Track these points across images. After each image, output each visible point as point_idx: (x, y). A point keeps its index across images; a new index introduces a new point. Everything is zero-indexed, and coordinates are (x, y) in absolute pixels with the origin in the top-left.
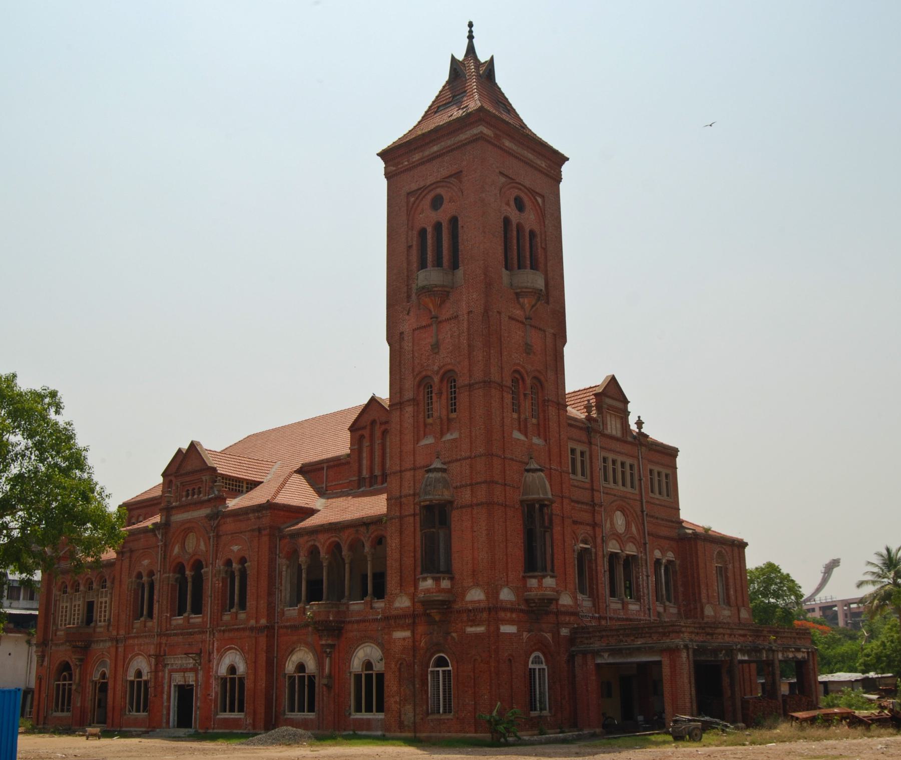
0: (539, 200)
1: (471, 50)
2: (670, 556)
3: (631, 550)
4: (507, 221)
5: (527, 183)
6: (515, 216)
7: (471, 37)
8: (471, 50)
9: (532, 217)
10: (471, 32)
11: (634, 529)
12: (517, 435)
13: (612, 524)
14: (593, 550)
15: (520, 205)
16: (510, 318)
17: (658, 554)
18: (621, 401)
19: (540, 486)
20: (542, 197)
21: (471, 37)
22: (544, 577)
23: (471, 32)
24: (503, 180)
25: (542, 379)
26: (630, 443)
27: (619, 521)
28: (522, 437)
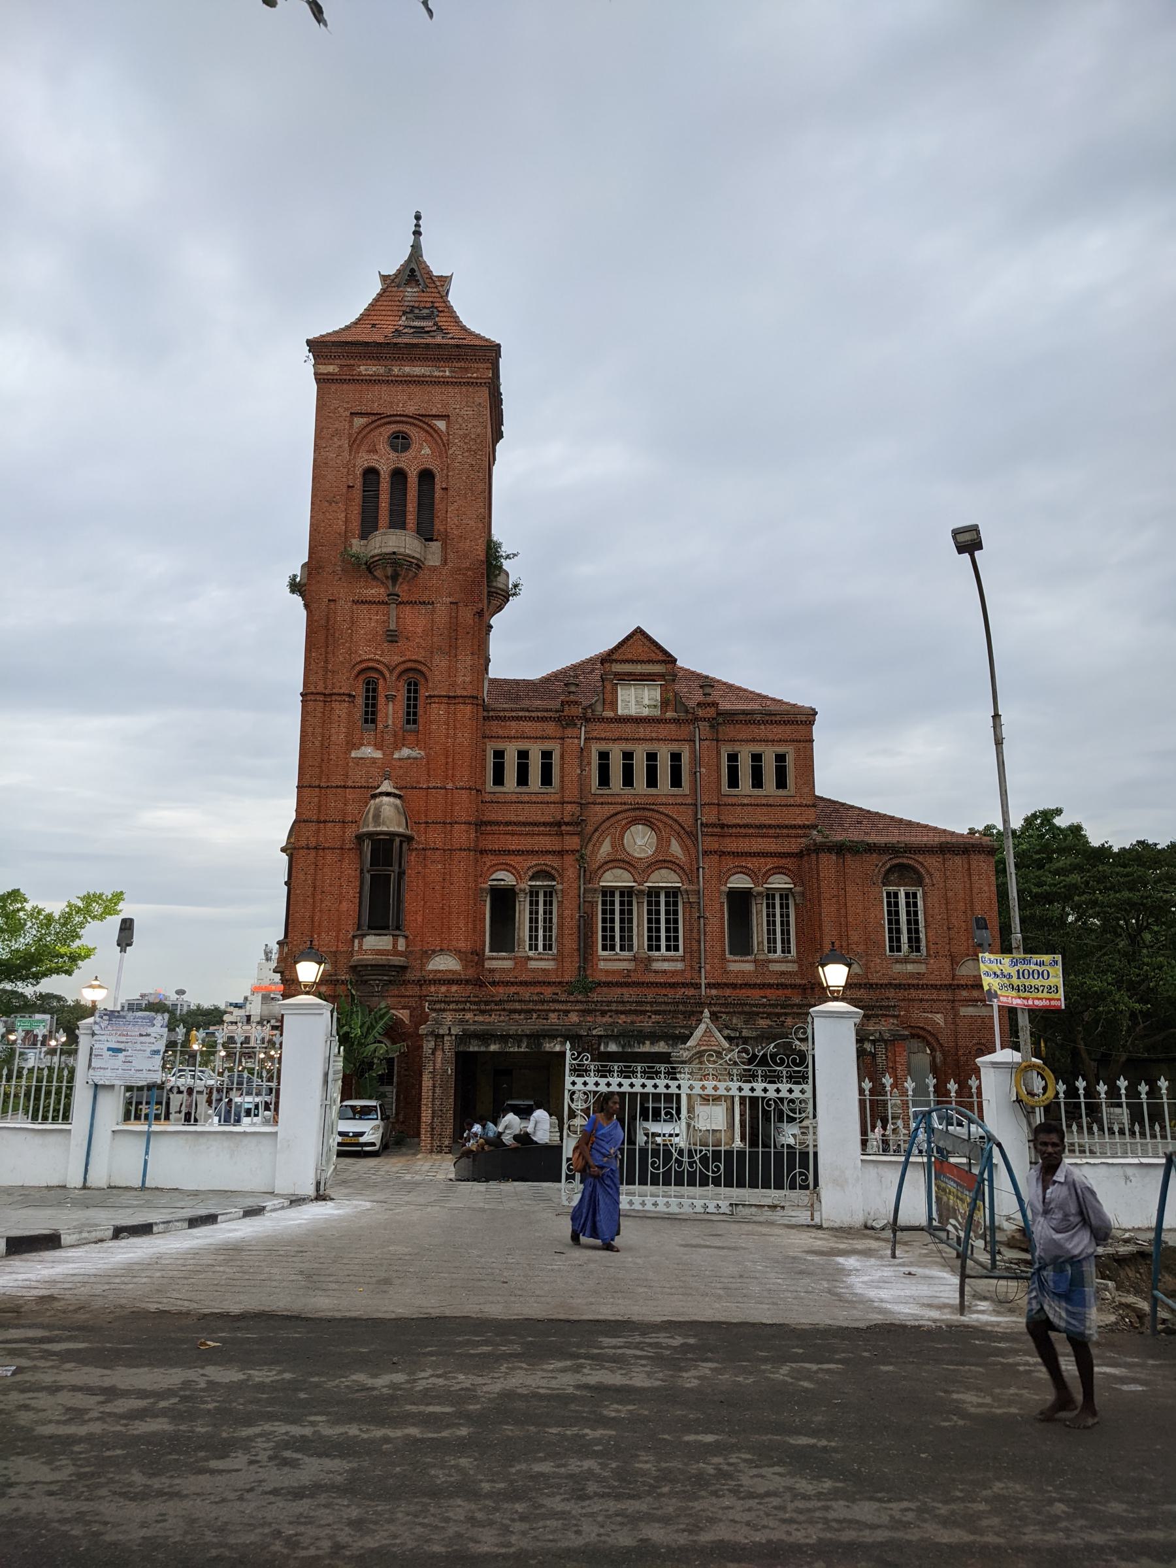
0: (441, 425)
1: (416, 249)
2: (779, 882)
3: (665, 879)
4: (371, 473)
5: (411, 409)
6: (385, 461)
7: (417, 233)
8: (416, 249)
9: (426, 451)
10: (418, 225)
11: (676, 848)
12: (368, 751)
13: (618, 844)
14: (559, 887)
15: (400, 442)
16: (354, 602)
17: (740, 882)
18: (663, 661)
19: (387, 815)
20: (445, 417)
21: (417, 233)
22: (364, 936)
23: (418, 225)
24: (359, 422)
25: (424, 669)
26: (675, 721)
27: (641, 841)
28: (378, 754)
